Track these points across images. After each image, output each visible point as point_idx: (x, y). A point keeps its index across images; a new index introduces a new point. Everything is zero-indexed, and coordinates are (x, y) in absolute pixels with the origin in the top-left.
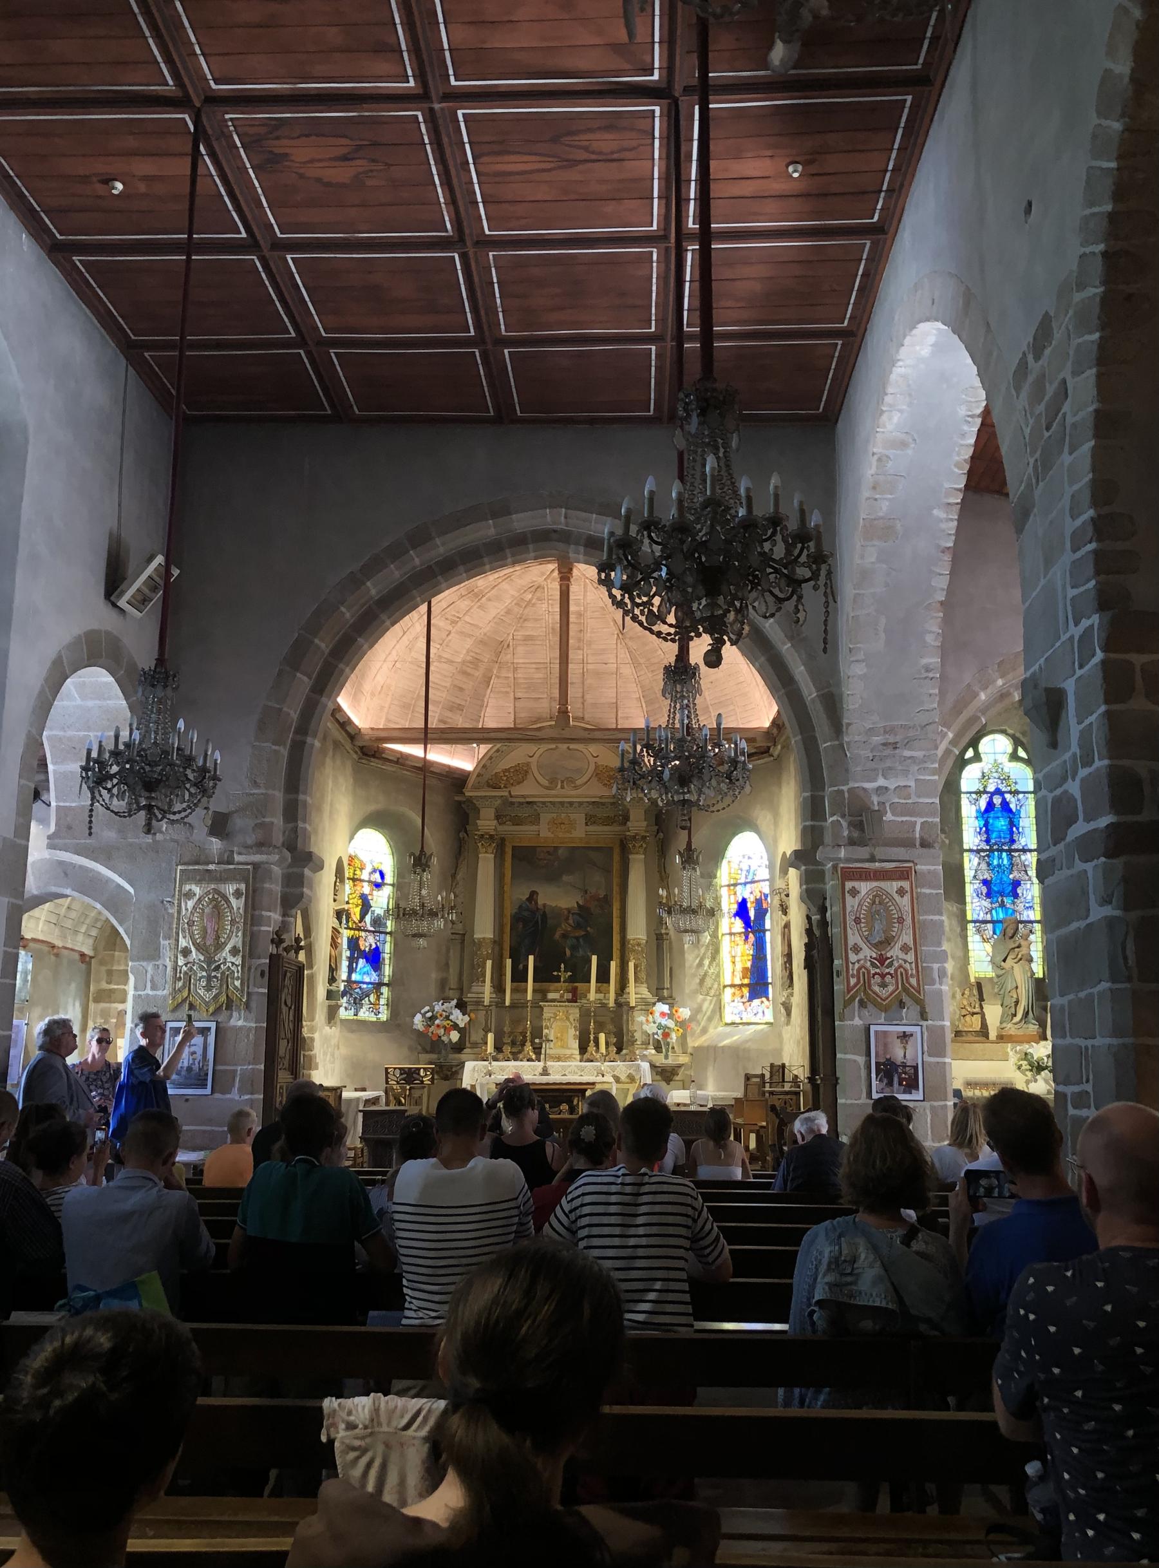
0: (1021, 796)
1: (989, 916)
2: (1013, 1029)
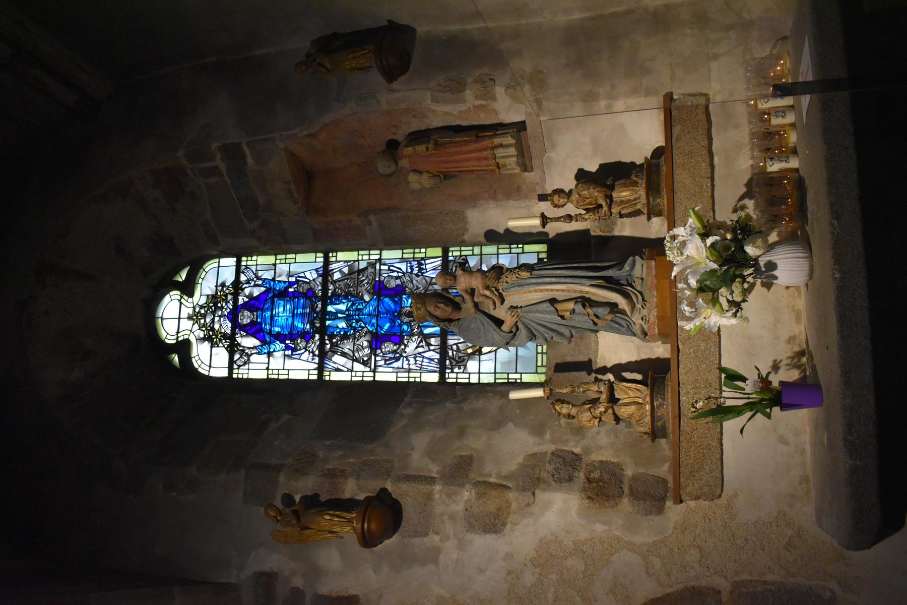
0: (243, 278)
1: (433, 341)
2: (644, 312)
